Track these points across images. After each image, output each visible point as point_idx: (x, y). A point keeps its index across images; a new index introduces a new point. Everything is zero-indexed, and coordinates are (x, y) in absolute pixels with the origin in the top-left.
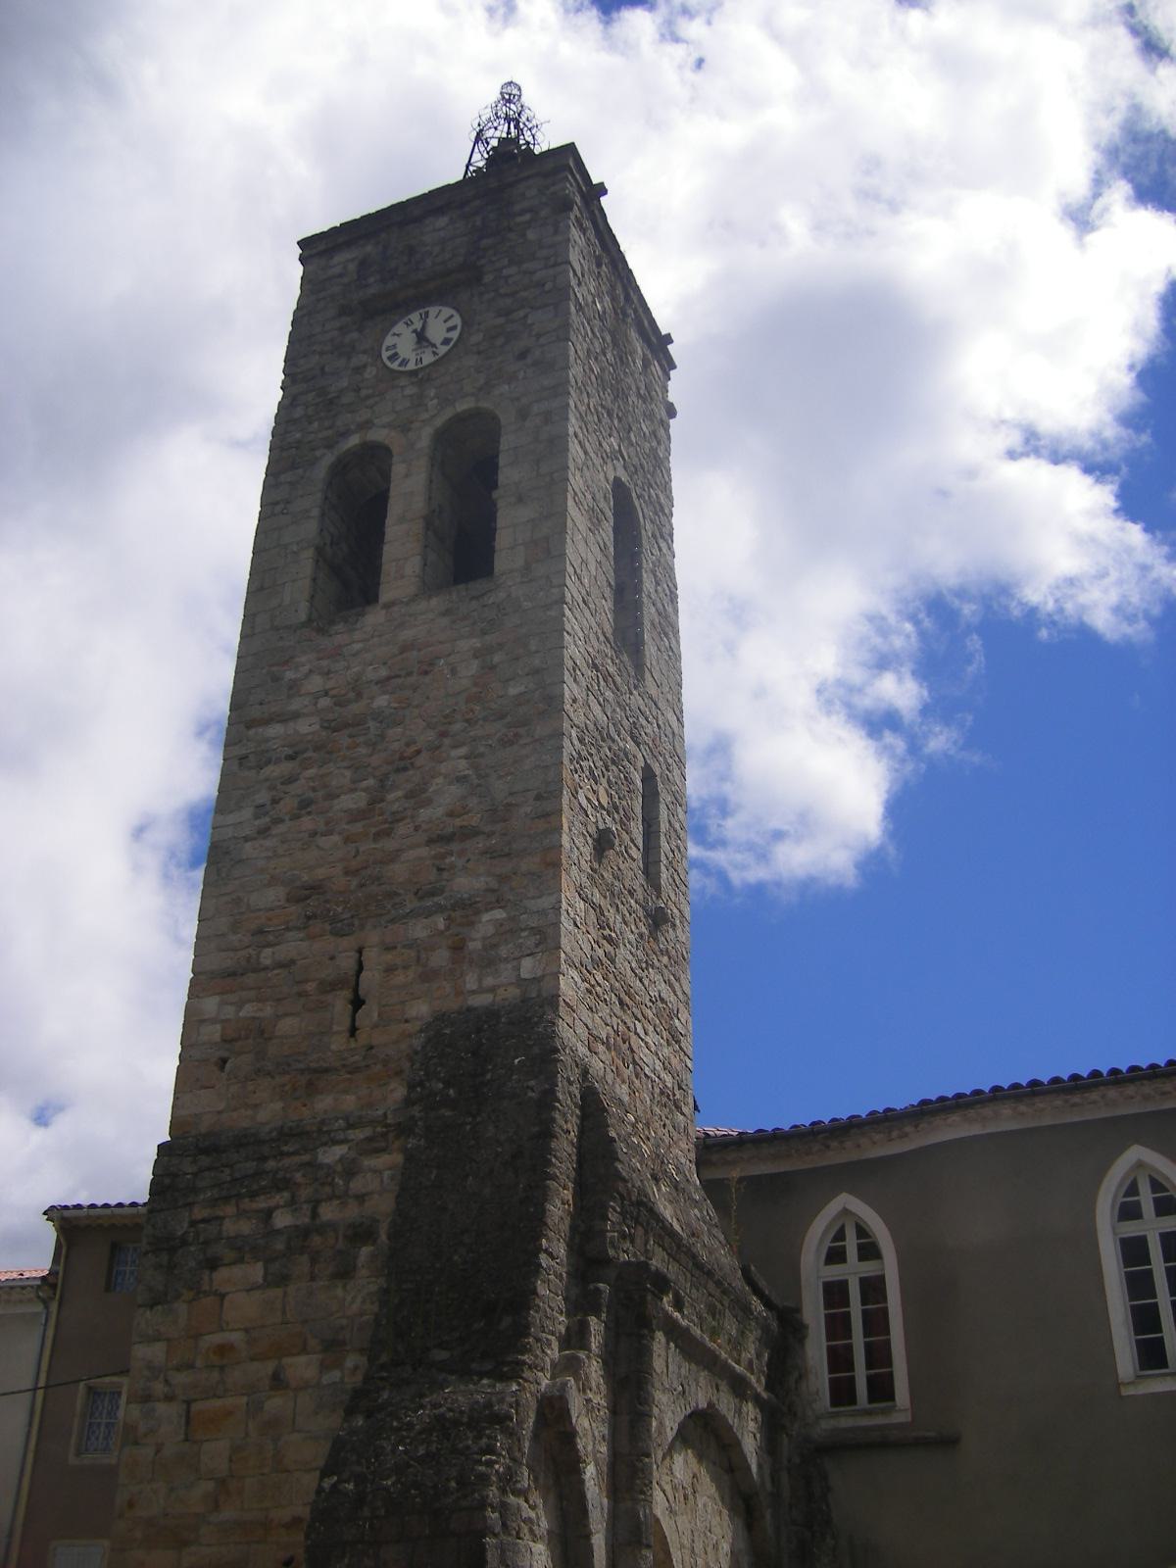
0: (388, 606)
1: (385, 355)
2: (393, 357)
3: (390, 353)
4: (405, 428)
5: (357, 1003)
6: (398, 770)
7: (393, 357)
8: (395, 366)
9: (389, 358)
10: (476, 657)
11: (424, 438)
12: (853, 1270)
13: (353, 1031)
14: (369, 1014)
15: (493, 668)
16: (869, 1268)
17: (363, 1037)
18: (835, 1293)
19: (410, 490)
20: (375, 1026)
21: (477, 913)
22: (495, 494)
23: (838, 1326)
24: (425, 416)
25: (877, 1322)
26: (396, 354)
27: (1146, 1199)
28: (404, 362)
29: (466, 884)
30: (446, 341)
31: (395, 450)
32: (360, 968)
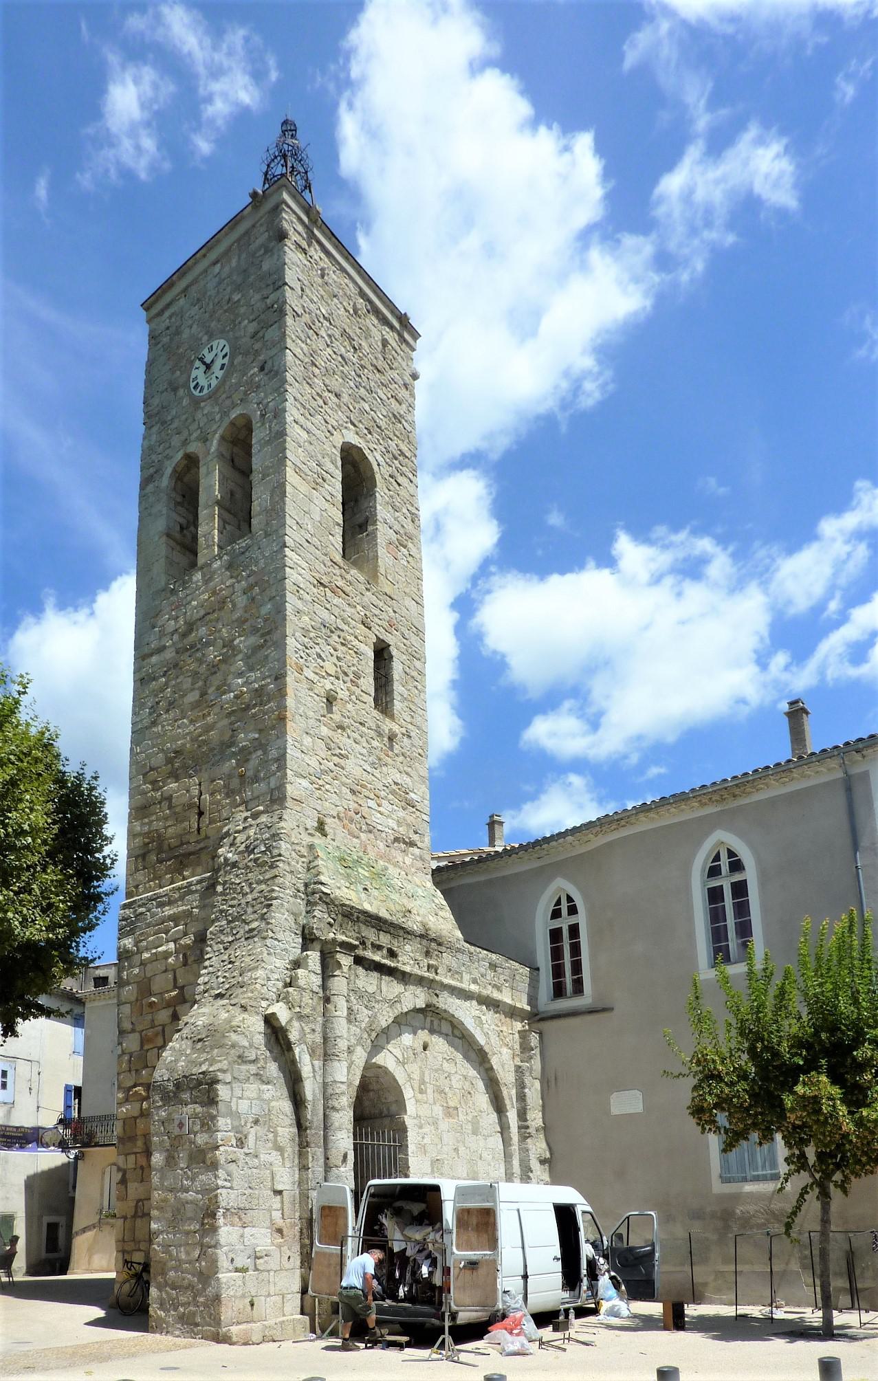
0: (202, 568)
4: (205, 440)
18: (555, 935)
19: (212, 483)
21: (250, 753)
23: (556, 954)
25: (576, 950)
27: (724, 863)
29: (243, 739)
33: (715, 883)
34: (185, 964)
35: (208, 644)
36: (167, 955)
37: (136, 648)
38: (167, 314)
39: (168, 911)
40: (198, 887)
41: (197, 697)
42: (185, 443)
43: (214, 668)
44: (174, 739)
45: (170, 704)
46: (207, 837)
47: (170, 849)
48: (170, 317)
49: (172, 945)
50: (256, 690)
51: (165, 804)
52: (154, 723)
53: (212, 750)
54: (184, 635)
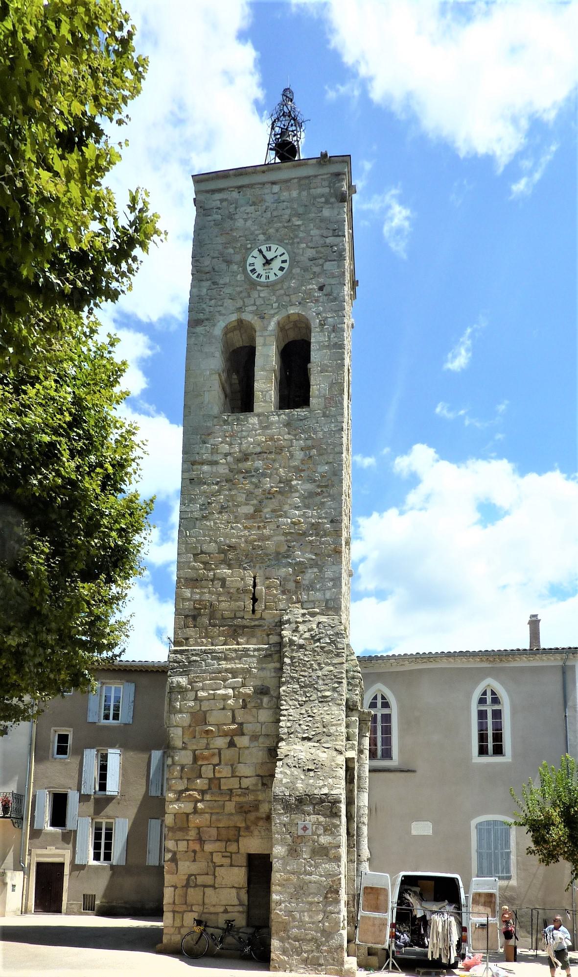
1: (249, 268)
2: (253, 271)
3: (252, 268)
5: (255, 600)
6: (267, 498)
7: (253, 271)
8: (254, 276)
9: (252, 271)
10: (302, 450)
11: (272, 325)
12: (379, 712)
13: (254, 611)
14: (260, 606)
15: (310, 457)
16: (386, 711)
17: (258, 615)
20: (264, 610)
21: (306, 568)
22: (309, 366)
24: (272, 312)
26: (254, 269)
28: (259, 276)
29: (300, 556)
30: (282, 269)
31: (257, 328)
32: (255, 586)
33: (483, 708)
34: (244, 707)
35: (264, 475)
36: (225, 698)
37: (185, 452)
38: (218, 196)
39: (224, 665)
40: (256, 653)
41: (252, 511)
42: (240, 310)
43: (269, 495)
44: (226, 536)
45: (222, 507)
46: (261, 618)
47: (223, 618)
48: (222, 201)
49: (230, 691)
50: (313, 524)
51: (218, 584)
52: (204, 518)
53: (267, 555)
54: (239, 460)
